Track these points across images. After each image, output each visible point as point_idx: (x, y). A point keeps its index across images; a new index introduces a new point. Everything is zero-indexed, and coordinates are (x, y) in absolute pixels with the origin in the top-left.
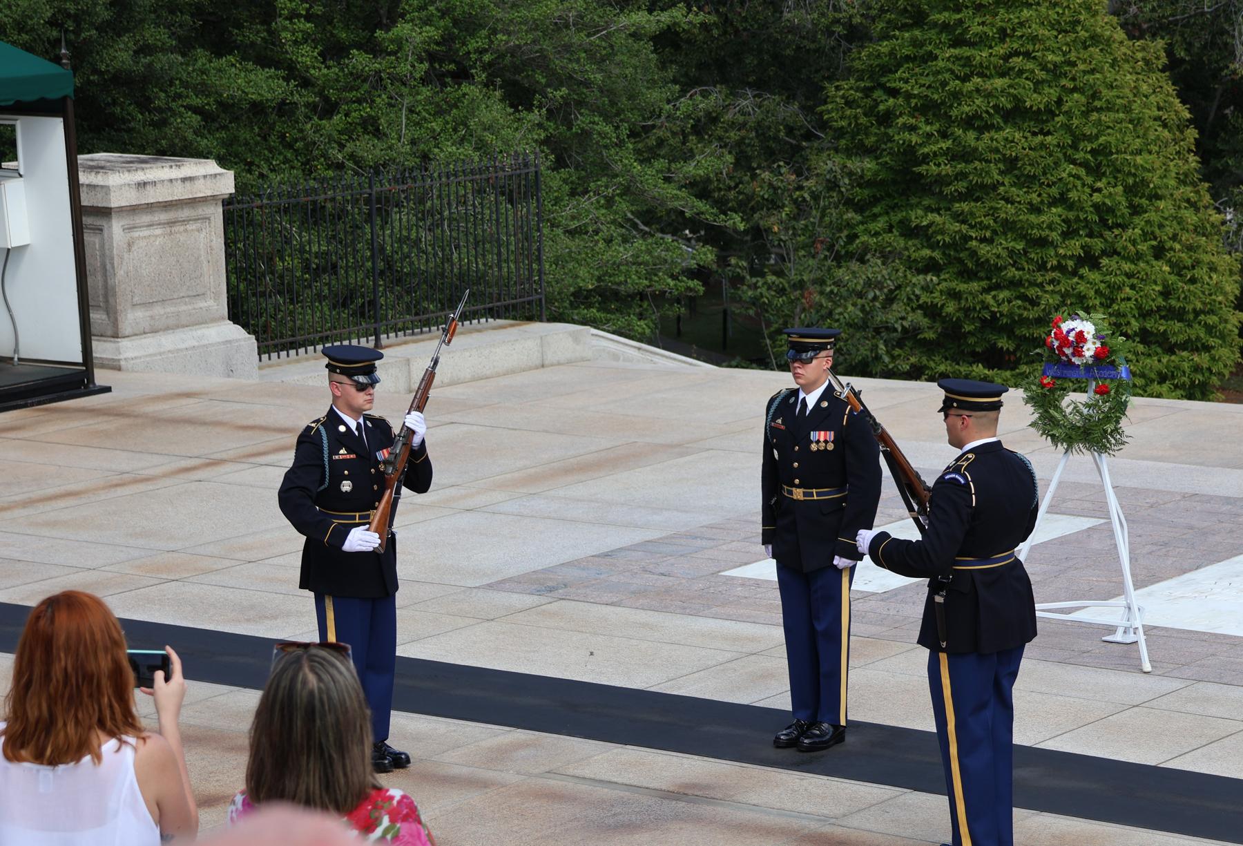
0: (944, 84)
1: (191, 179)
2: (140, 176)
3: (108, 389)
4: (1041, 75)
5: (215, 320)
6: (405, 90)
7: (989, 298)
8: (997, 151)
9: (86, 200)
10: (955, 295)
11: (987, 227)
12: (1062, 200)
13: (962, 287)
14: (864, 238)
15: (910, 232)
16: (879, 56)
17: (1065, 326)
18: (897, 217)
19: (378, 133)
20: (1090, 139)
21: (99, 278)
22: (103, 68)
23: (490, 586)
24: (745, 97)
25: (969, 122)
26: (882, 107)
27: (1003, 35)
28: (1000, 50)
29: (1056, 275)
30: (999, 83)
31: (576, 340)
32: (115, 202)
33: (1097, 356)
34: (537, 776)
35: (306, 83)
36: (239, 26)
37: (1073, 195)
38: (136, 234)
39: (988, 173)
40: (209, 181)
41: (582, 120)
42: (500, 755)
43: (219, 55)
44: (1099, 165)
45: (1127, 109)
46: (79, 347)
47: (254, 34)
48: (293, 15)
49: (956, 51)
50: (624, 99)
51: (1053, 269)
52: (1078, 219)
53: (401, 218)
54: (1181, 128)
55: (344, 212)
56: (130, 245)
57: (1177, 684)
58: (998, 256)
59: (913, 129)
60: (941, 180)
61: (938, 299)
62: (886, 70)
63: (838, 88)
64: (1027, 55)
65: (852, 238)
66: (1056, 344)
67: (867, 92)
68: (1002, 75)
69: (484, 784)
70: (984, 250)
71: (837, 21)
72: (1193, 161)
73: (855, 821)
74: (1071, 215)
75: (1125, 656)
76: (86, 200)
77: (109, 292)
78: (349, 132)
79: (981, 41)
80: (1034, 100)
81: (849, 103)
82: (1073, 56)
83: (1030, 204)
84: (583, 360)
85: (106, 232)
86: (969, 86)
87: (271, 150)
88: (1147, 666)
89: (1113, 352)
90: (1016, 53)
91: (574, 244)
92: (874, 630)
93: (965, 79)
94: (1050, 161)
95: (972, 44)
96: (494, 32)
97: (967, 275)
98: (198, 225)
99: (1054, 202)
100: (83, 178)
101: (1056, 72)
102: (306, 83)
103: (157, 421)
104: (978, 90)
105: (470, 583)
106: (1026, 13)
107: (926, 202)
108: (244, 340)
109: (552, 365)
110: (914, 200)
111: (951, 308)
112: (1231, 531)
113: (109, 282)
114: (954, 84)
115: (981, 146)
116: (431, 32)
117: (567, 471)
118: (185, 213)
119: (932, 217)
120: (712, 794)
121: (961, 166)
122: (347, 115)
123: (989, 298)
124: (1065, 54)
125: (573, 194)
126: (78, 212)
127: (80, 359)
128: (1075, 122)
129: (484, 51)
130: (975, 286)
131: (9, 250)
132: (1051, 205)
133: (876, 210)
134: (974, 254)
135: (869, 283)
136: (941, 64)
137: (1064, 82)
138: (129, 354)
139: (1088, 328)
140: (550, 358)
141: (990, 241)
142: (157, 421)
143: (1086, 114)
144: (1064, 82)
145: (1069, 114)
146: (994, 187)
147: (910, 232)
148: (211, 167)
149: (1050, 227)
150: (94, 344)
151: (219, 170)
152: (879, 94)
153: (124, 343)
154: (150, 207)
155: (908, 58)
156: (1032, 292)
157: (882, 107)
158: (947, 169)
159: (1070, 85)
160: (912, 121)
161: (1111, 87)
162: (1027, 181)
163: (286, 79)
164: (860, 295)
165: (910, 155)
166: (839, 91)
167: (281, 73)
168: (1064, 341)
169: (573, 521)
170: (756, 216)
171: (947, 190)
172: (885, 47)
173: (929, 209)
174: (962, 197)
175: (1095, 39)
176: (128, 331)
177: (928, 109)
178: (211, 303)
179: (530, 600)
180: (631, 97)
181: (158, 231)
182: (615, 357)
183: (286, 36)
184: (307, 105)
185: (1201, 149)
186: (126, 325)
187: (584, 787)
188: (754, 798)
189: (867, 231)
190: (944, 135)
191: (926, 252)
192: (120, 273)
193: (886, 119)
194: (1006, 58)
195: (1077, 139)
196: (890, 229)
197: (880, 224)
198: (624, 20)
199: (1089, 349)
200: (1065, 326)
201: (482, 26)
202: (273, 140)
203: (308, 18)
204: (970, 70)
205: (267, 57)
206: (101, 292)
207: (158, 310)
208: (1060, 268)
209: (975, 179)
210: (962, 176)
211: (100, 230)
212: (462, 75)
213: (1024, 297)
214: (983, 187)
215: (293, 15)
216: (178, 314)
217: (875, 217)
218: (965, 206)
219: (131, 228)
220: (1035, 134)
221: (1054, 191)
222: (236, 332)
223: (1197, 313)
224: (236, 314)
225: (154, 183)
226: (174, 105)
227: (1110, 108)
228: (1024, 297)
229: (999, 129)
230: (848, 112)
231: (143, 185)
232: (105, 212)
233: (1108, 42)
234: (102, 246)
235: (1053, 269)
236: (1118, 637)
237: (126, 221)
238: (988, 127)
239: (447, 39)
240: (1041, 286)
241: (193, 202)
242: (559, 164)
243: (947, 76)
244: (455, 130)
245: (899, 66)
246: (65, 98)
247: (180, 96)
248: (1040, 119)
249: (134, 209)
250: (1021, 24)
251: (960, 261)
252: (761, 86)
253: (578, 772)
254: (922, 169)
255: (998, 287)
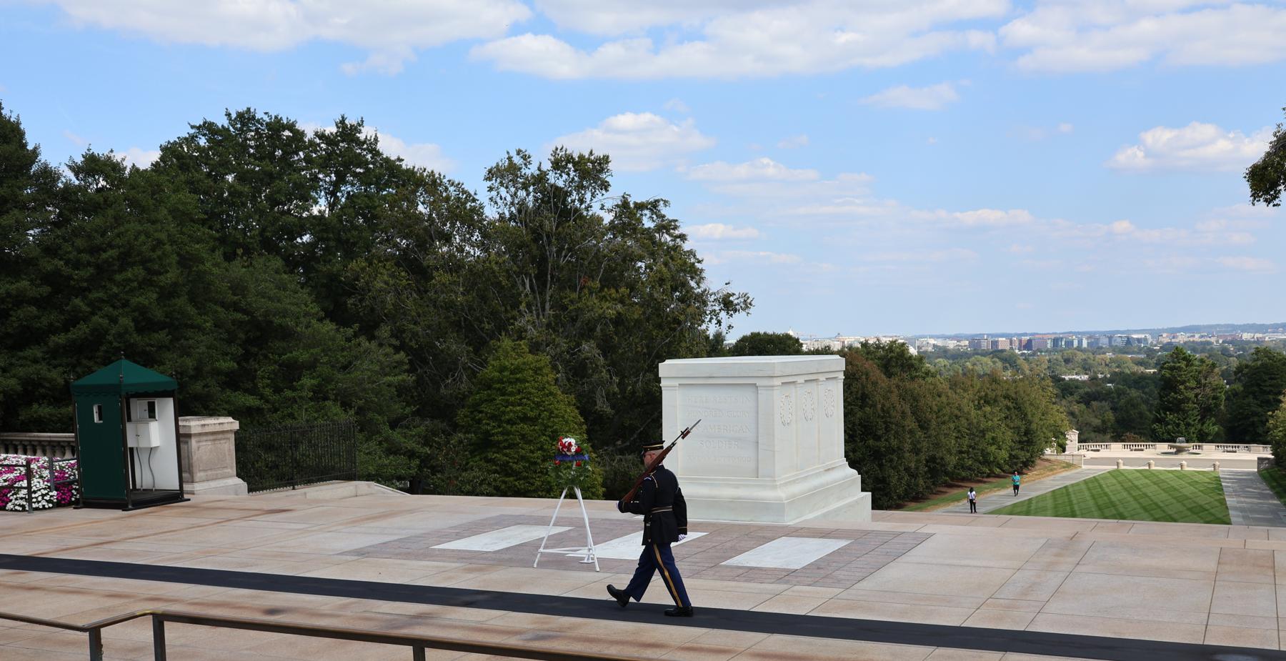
0: (499, 409)
1: (222, 423)
2: (203, 422)
3: (189, 500)
4: (533, 406)
5: (231, 476)
6: (304, 402)
7: (517, 483)
8: (518, 432)
9: (181, 431)
10: (505, 482)
11: (515, 458)
12: (541, 449)
13: (507, 479)
14: (471, 463)
15: (488, 461)
16: (476, 399)
17: (564, 441)
18: (483, 456)
19: (295, 418)
20: (551, 427)
21: (187, 460)
22: (191, 392)
23: (338, 554)
24: (427, 420)
25: (509, 422)
26: (477, 418)
27: (519, 392)
28: (518, 397)
29: (540, 475)
30: (518, 408)
31: (369, 486)
32: (193, 431)
33: (576, 451)
34: (361, 612)
35: (267, 401)
36: (243, 383)
37: (545, 447)
38: (201, 444)
39: (515, 439)
40: (229, 425)
41: (370, 415)
42: (344, 607)
43: (235, 391)
44: (554, 437)
45: (563, 417)
46: (178, 484)
47: (249, 385)
48: (263, 377)
49: (503, 398)
50: (385, 408)
51: (539, 472)
52: (547, 455)
53: (302, 448)
54: (581, 424)
55: (281, 446)
56: (199, 448)
57: (609, 575)
58: (519, 468)
59: (488, 424)
60: (499, 442)
61: (498, 484)
62: (478, 405)
63: (462, 412)
64: (528, 399)
65: (467, 463)
66: (561, 447)
67: (472, 412)
68: (519, 406)
69: (338, 616)
70: (515, 466)
71: (459, 393)
72: (585, 436)
73: (492, 622)
74: (545, 454)
75: (590, 567)
76: (181, 431)
77: (190, 466)
78: (283, 418)
79: (512, 394)
80: (531, 414)
81: (465, 417)
82: (544, 399)
83: (530, 450)
84: (372, 494)
85: (189, 443)
86: (508, 409)
87: (254, 425)
88: (598, 569)
89: (582, 450)
90: (525, 398)
91: (367, 458)
92: (491, 562)
93: (506, 407)
94: (537, 435)
95: (509, 395)
96: (337, 382)
97: (510, 475)
98: (224, 441)
99: (539, 449)
100: (180, 423)
101: (538, 405)
102: (267, 401)
103: (207, 509)
104: (511, 411)
105: (331, 553)
106: (527, 384)
107: (493, 450)
108: (243, 485)
109: (360, 496)
110: (489, 450)
111: (503, 487)
112: (621, 529)
113: (191, 461)
114: (502, 409)
115: (513, 430)
116: (314, 382)
117: (368, 519)
118: (220, 436)
119: (495, 455)
120: (434, 616)
121: (506, 437)
122: (283, 412)
123: (517, 483)
124: (541, 398)
125: (367, 441)
126: (178, 436)
127: (178, 489)
128: (545, 422)
129: (334, 389)
130: (512, 479)
131: (151, 448)
132: (537, 450)
133: (476, 453)
134: (511, 468)
135: (474, 477)
136: (498, 402)
137: (541, 408)
138: (198, 489)
139: (573, 441)
140: (359, 493)
141: (516, 463)
142: (207, 509)
143: (549, 419)
144: (541, 408)
145: (543, 419)
146: (518, 444)
147: (488, 461)
148: (230, 419)
149: (537, 458)
150: (184, 485)
151: (233, 420)
152: (476, 413)
153: (196, 485)
154: (206, 434)
155: (486, 400)
156: (531, 481)
157: (477, 418)
158: (501, 438)
159: (543, 409)
160: (488, 422)
161: (557, 410)
162: (529, 442)
163: (260, 399)
164: (472, 481)
165: (488, 431)
166: (462, 412)
167: (258, 397)
168: (564, 445)
169: (371, 534)
170: (432, 462)
171: (502, 446)
172: (478, 397)
173: (494, 453)
174: (505, 448)
175: (551, 393)
176: (197, 480)
177: (493, 417)
178: (229, 470)
179: (356, 558)
180: (388, 407)
181: (210, 443)
182: (384, 493)
183: (260, 385)
184: (268, 409)
185: (588, 432)
186: (196, 479)
187: (379, 616)
188: (448, 617)
189: (473, 461)
190: (499, 427)
191: (494, 467)
192: (195, 458)
193: (479, 421)
194: (520, 399)
195: (546, 427)
196: (481, 460)
197: (478, 458)
198: (385, 379)
199: (573, 449)
200: (564, 441)
201: (332, 381)
202: (255, 423)
203: (268, 379)
204: (508, 403)
205: (253, 391)
206: (187, 466)
207: (209, 473)
208: (541, 472)
209: (511, 442)
210: (506, 440)
211: (187, 442)
212: (326, 399)
213: (529, 483)
214: (514, 444)
215: (263, 377)
216: (217, 474)
217: (475, 456)
218: (508, 451)
219: (199, 442)
220: (531, 426)
221: (539, 445)
222: (240, 481)
223: (589, 488)
224: (238, 475)
225: (208, 425)
226: (217, 408)
227: (557, 416)
228: (529, 483)
229: (519, 424)
230: (465, 420)
231: (204, 425)
232: (189, 436)
233: (556, 394)
234: (188, 447)
235: (539, 472)
236: (586, 561)
237: (197, 439)
238: (515, 424)
239: (319, 385)
240: (535, 478)
241: (223, 432)
242: (361, 431)
243: (500, 406)
244: (323, 417)
245: (483, 403)
246: (173, 391)
247: (219, 405)
248: (533, 421)
249: (200, 434)
250: (526, 388)
251: (506, 470)
252: (433, 418)
253: (377, 611)
254: (490, 438)
255: (520, 479)
